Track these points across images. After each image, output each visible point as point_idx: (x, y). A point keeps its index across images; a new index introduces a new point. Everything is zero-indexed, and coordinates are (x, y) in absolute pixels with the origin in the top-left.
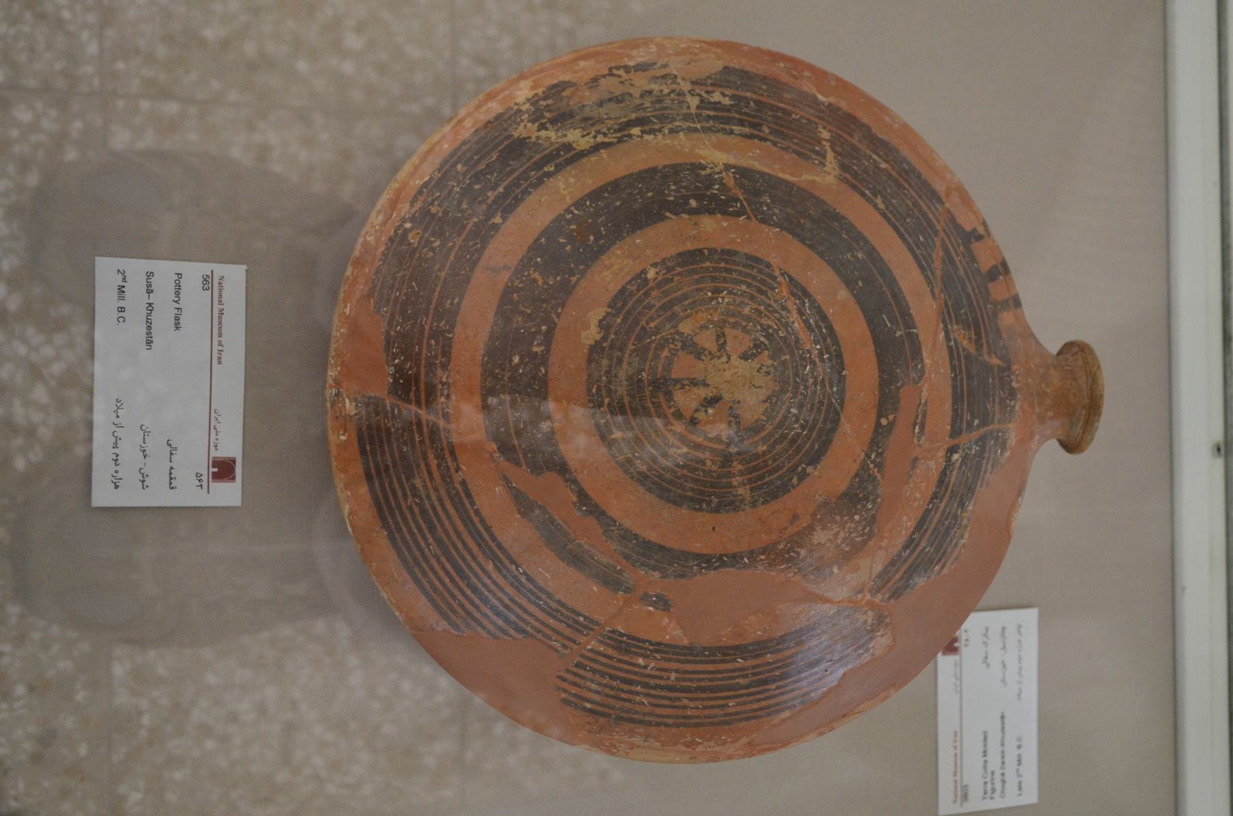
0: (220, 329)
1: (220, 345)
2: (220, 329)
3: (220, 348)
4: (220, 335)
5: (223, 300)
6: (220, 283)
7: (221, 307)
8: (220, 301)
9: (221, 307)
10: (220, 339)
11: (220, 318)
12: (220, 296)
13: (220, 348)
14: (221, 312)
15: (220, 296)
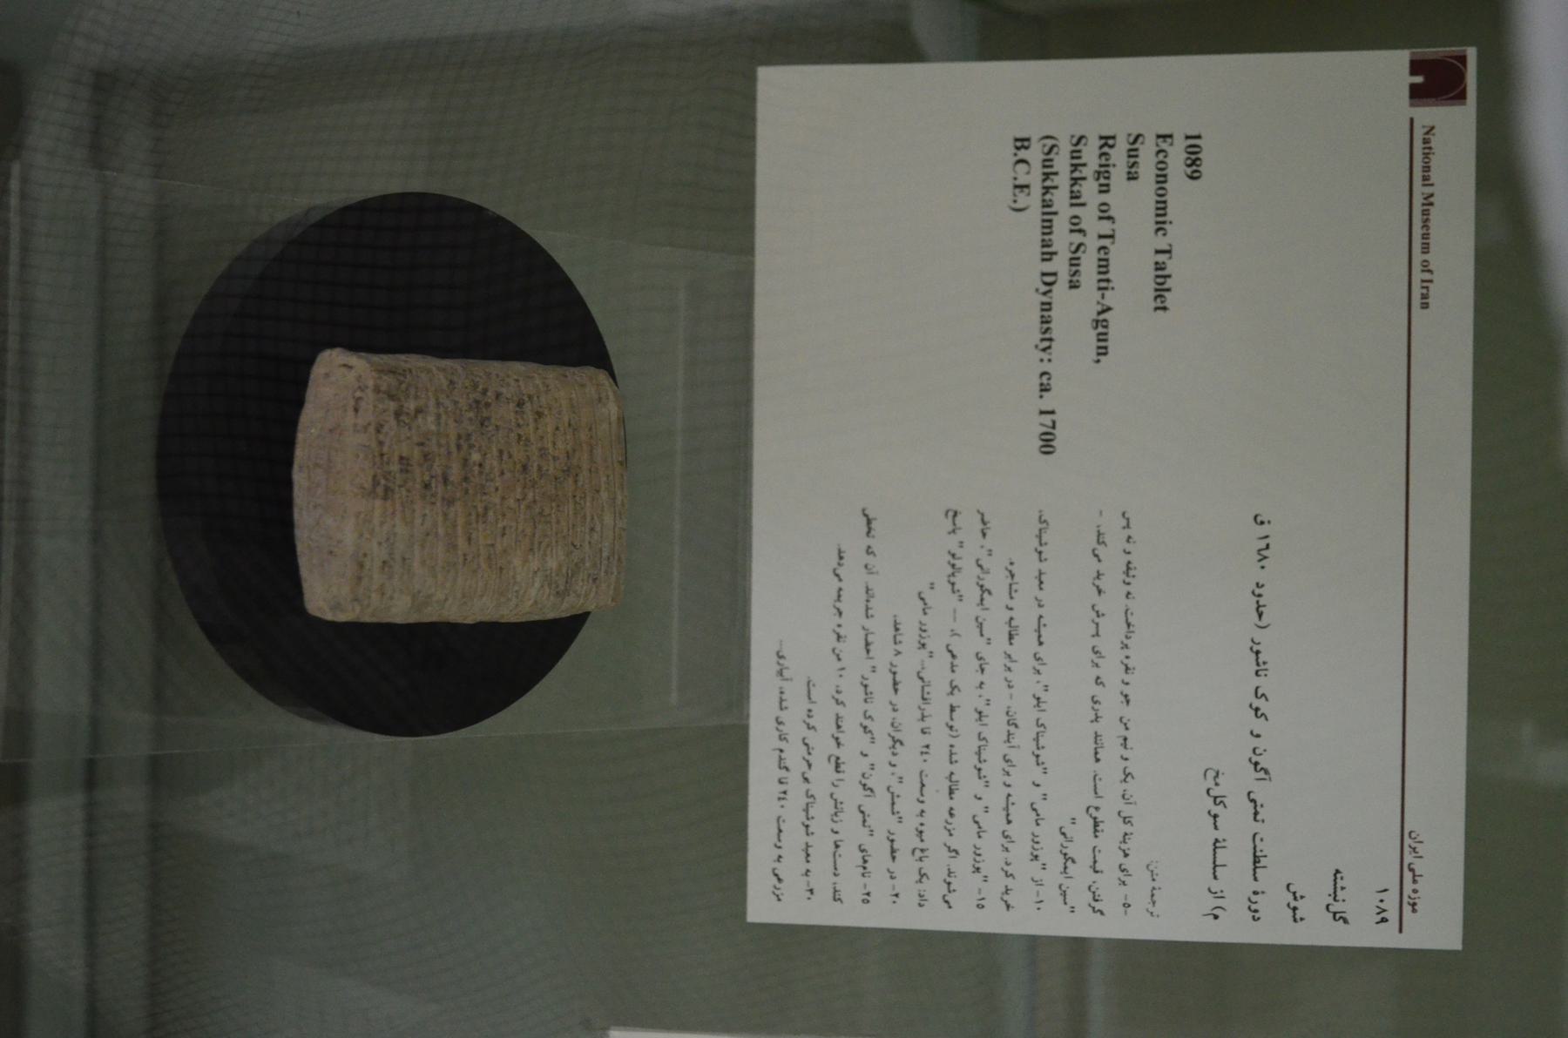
0: (1425, 236)
1: (1426, 268)
2: (1425, 236)
3: (1427, 276)
4: (1426, 249)
5: (1434, 176)
6: (1426, 141)
7: (1428, 190)
8: (1425, 178)
9: (1428, 190)
10: (1426, 257)
11: (1425, 213)
12: (1427, 168)
13: (1427, 276)
14: (1428, 201)
15: (1427, 168)
